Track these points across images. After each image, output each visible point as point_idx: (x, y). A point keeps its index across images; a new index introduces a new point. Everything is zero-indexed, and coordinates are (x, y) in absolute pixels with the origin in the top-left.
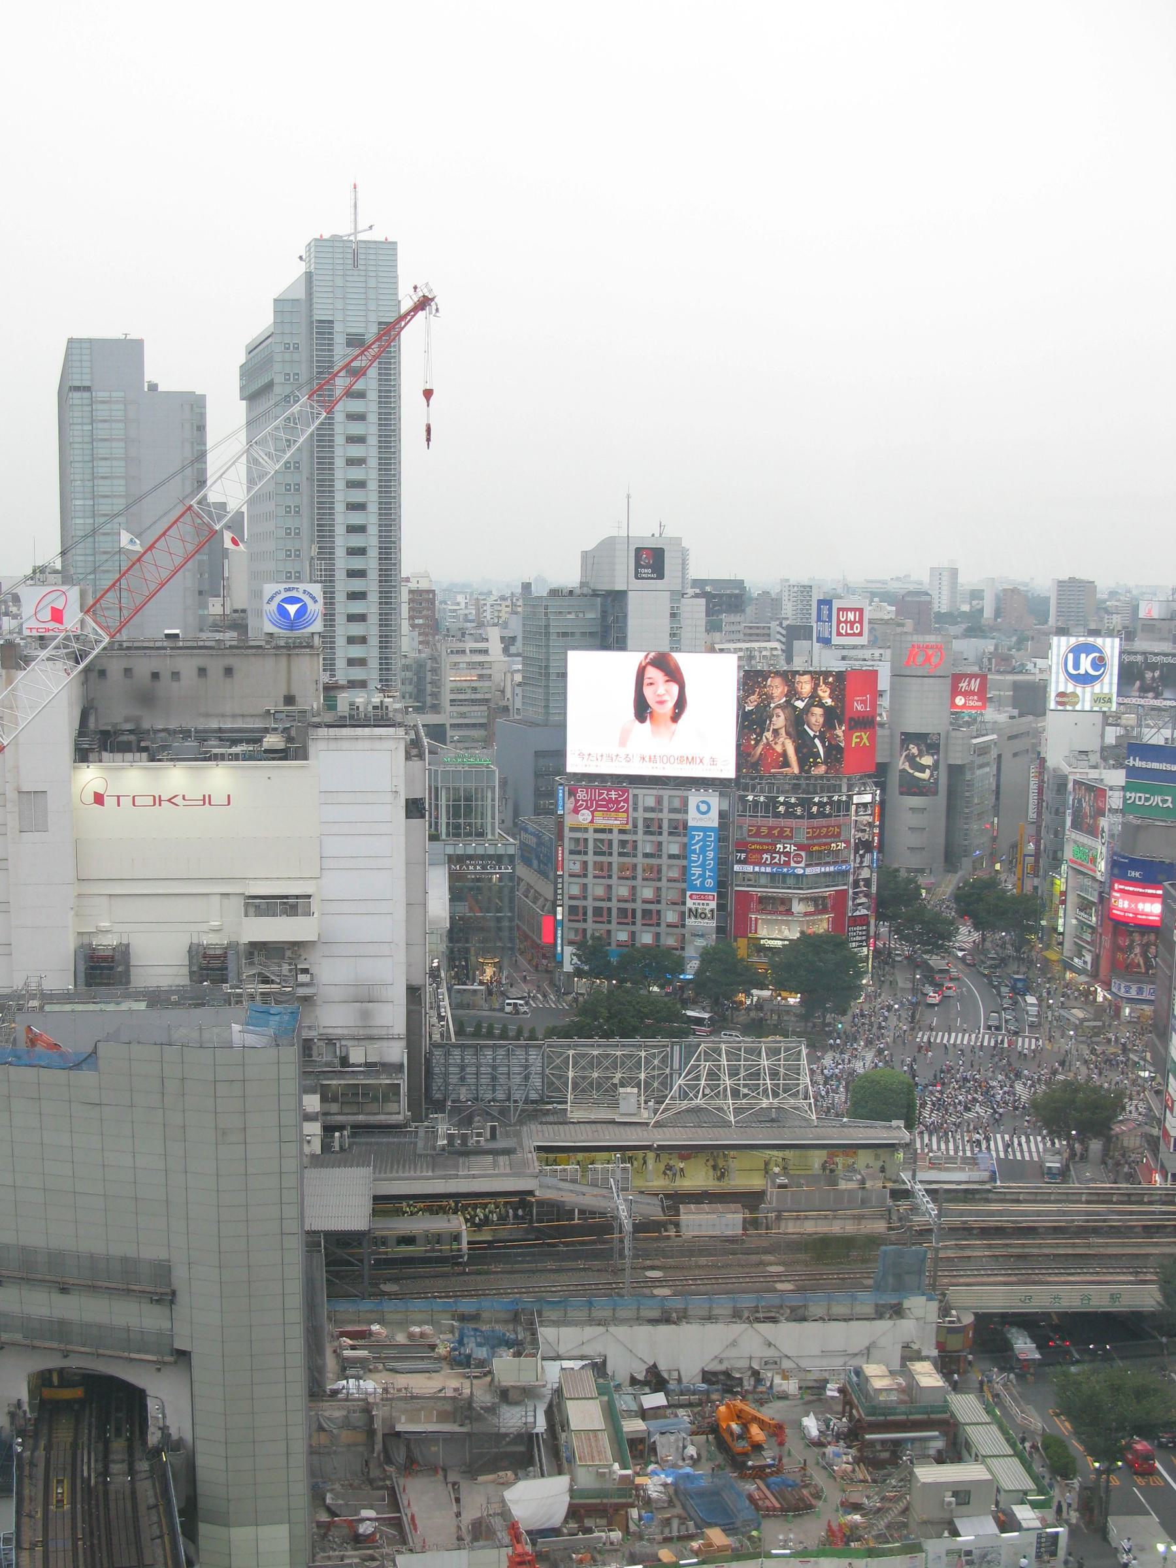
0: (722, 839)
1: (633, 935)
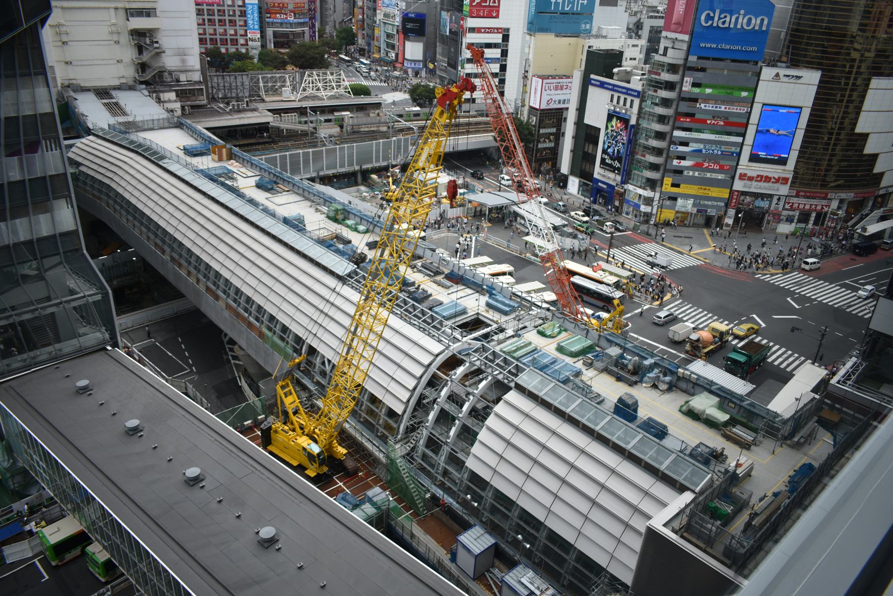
0: (260, 8)
1: (227, 49)
